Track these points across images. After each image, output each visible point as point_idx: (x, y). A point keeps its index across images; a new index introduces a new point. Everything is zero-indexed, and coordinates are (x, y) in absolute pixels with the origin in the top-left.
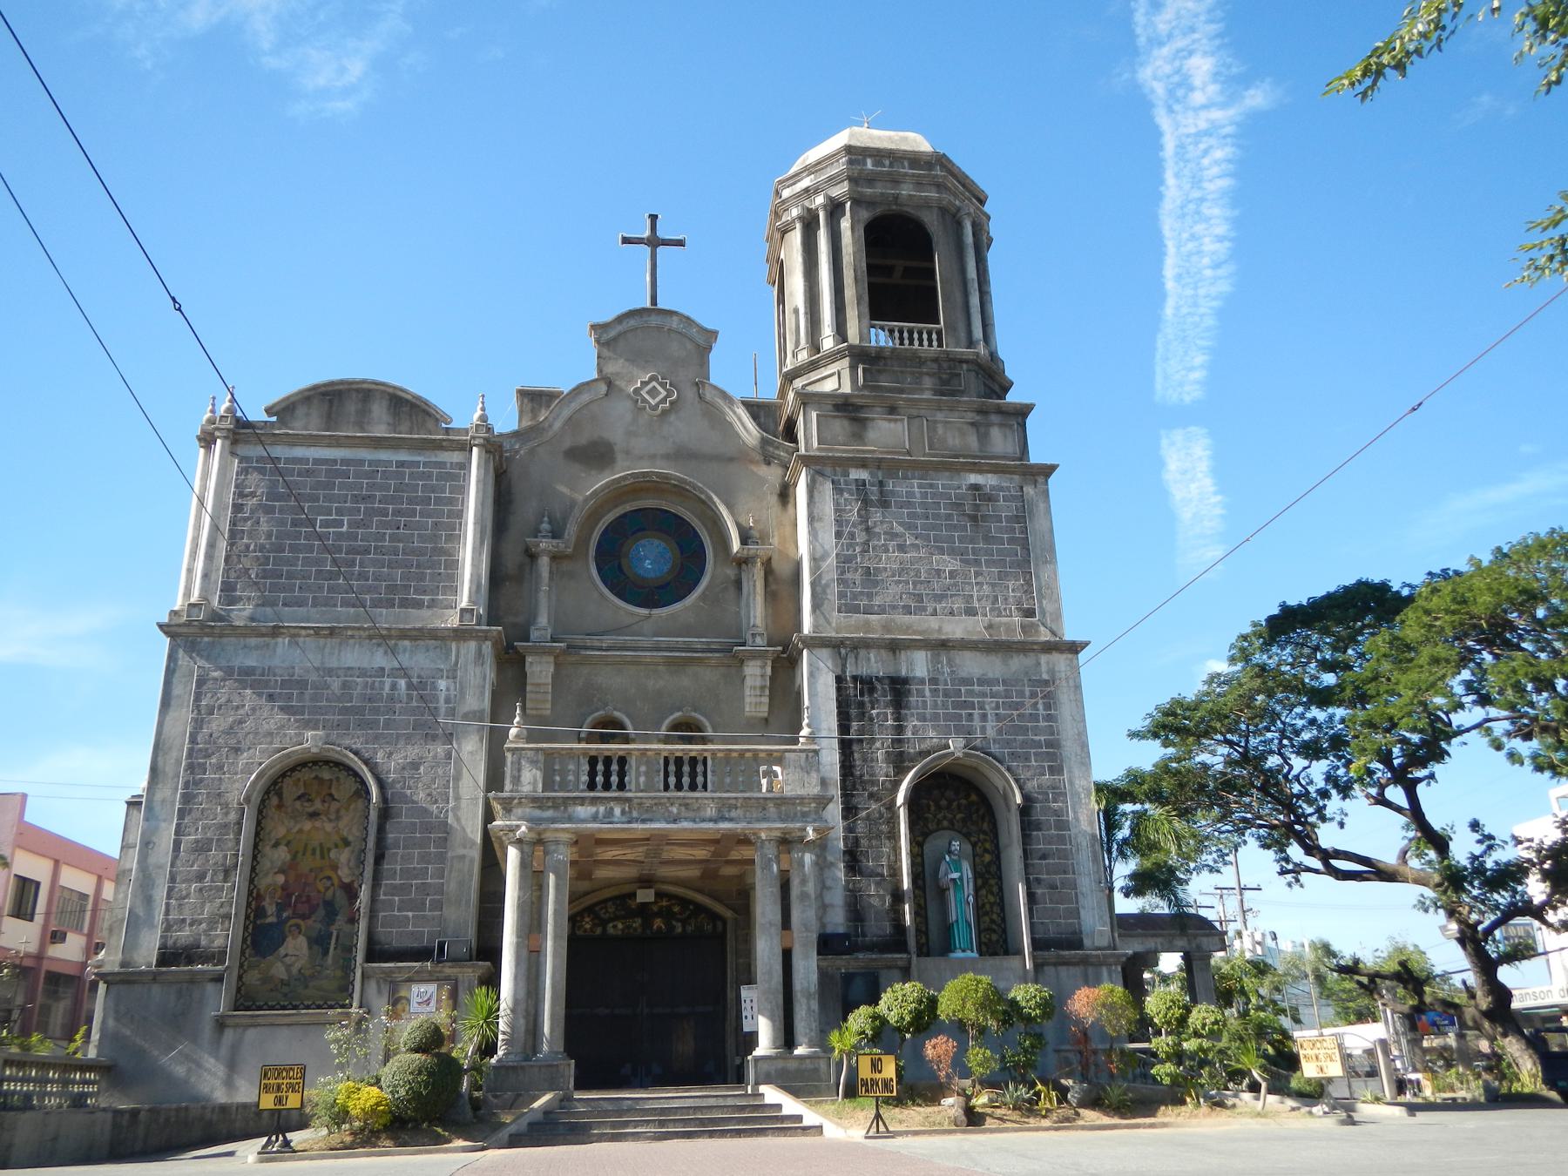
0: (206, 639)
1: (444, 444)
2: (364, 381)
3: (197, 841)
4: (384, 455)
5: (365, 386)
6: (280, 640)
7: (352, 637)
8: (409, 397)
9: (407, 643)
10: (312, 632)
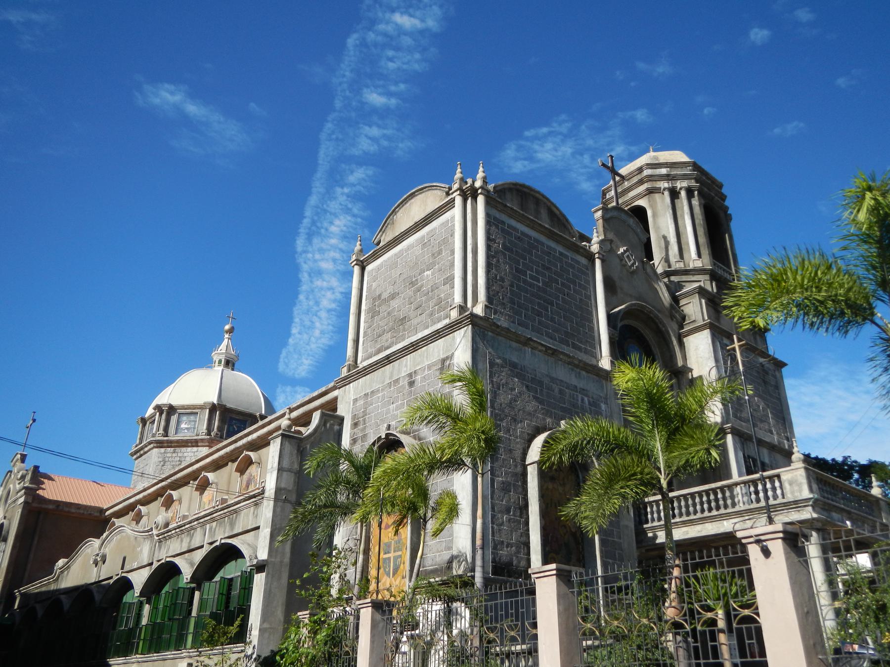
0: (490, 334)
1: (581, 250)
2: (538, 192)
3: (503, 483)
4: (553, 244)
5: (537, 195)
6: (526, 348)
7: (561, 360)
8: (558, 213)
9: (584, 373)
10: (544, 349)
